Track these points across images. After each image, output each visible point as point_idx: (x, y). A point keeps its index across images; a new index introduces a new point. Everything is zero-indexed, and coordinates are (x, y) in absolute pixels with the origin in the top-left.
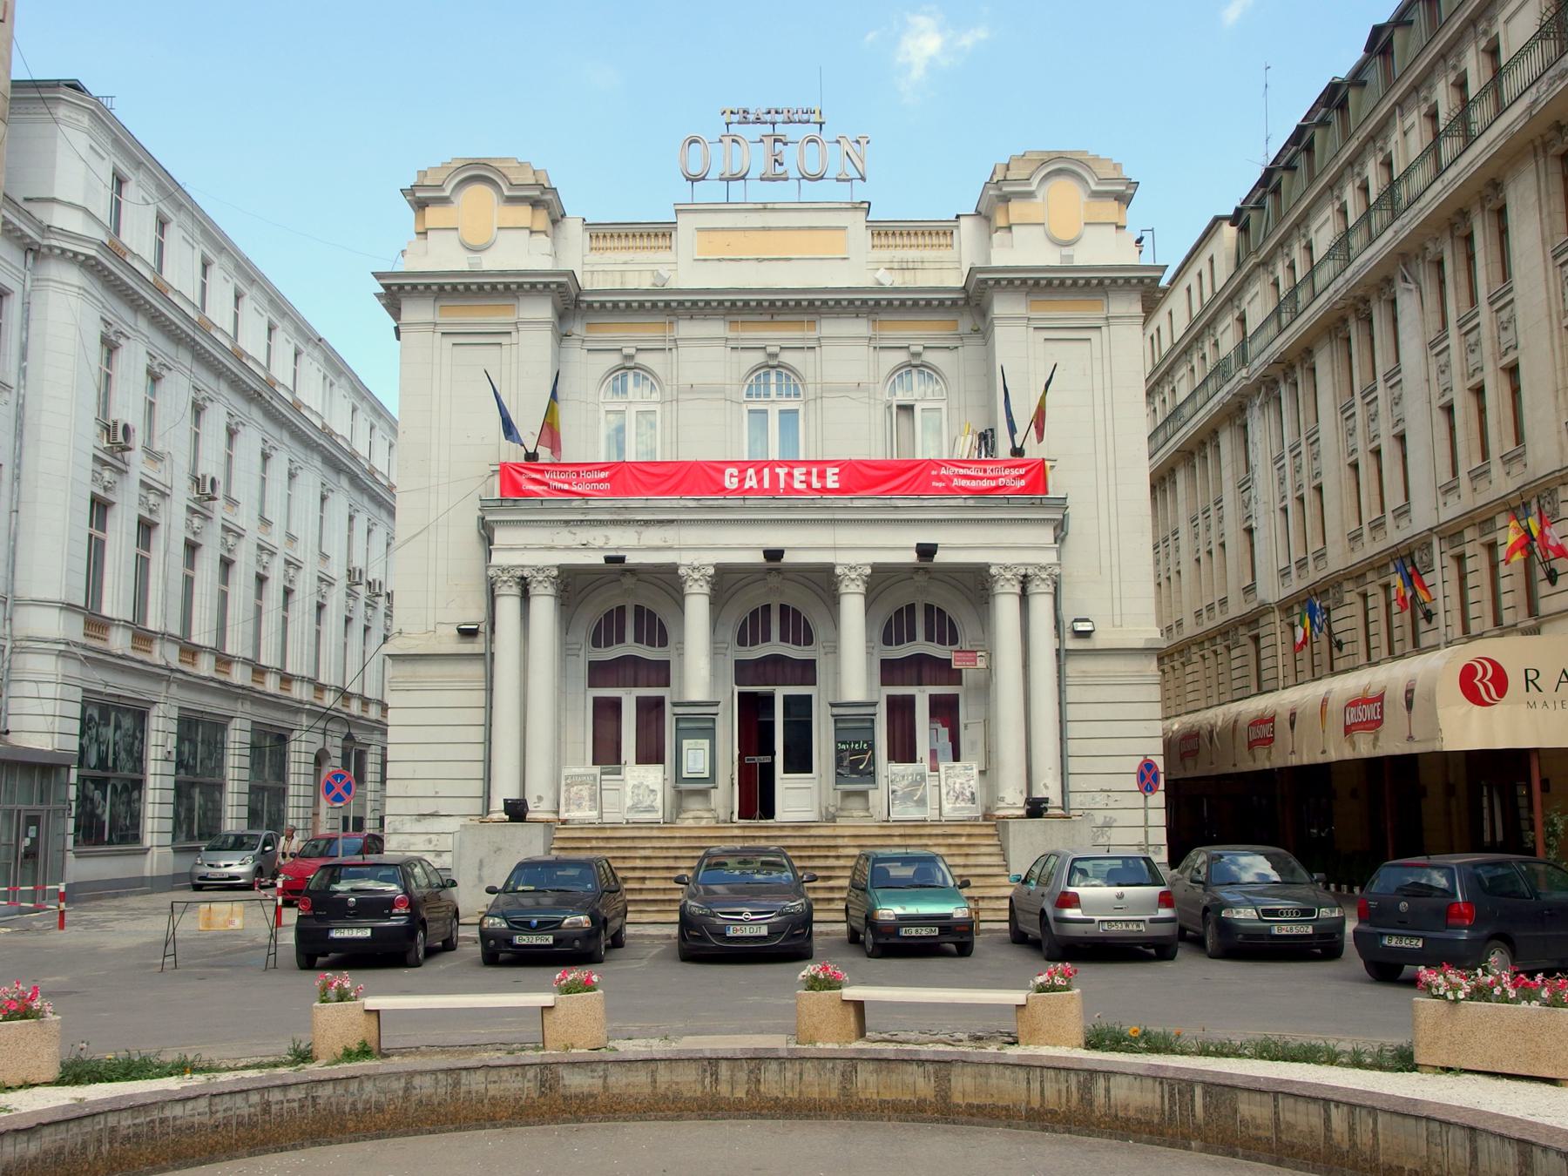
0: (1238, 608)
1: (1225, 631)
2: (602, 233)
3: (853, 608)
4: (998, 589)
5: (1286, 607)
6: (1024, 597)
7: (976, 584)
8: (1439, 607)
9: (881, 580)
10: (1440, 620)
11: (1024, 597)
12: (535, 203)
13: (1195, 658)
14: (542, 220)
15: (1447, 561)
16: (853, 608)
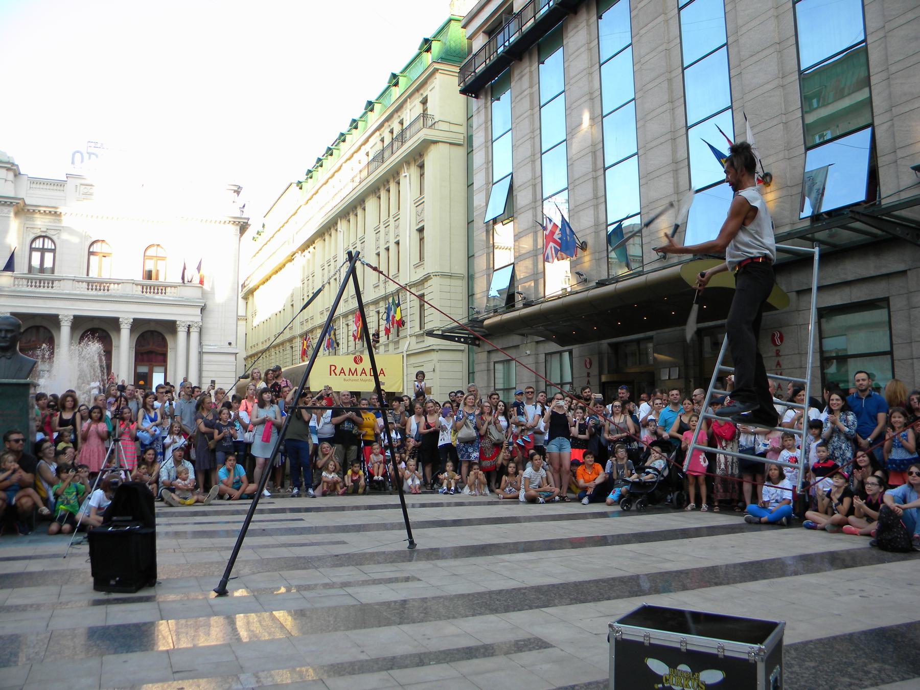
0: (287, 335)
1: (282, 343)
2: (35, 181)
3: (125, 332)
4: (179, 329)
5: (301, 336)
6: (188, 333)
7: (171, 326)
8: (341, 342)
9: (137, 324)
10: (341, 346)
11: (188, 333)
12: (8, 169)
13: (273, 354)
14: (10, 175)
15: (345, 326)
16: (125, 332)
